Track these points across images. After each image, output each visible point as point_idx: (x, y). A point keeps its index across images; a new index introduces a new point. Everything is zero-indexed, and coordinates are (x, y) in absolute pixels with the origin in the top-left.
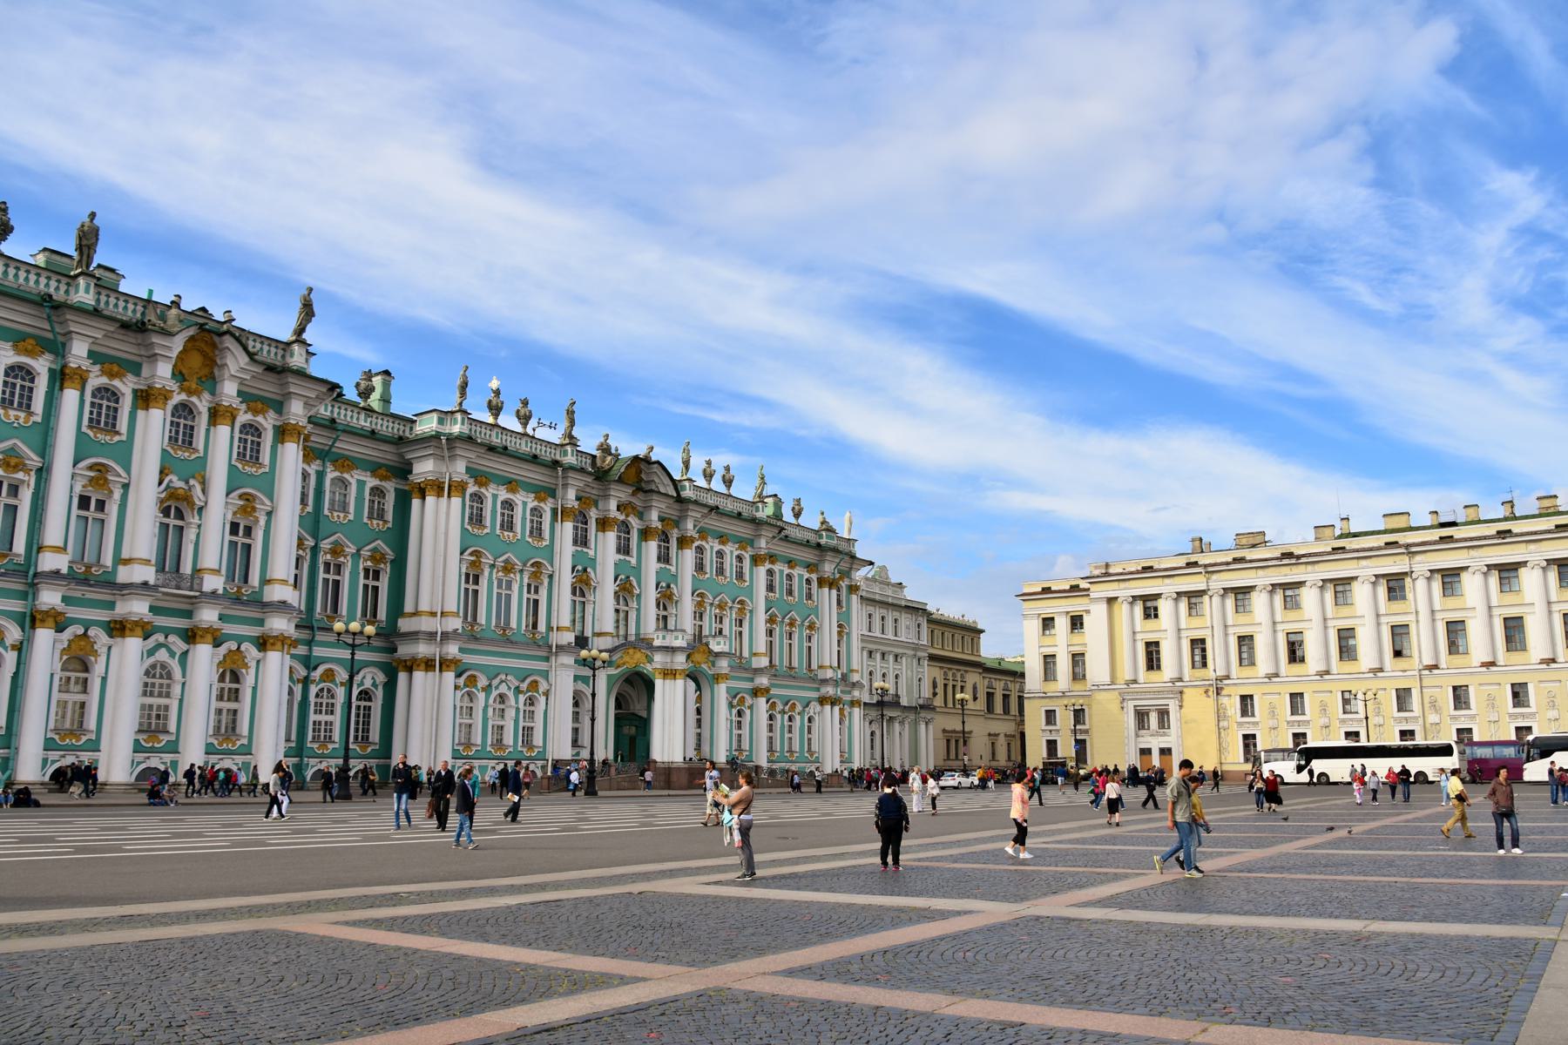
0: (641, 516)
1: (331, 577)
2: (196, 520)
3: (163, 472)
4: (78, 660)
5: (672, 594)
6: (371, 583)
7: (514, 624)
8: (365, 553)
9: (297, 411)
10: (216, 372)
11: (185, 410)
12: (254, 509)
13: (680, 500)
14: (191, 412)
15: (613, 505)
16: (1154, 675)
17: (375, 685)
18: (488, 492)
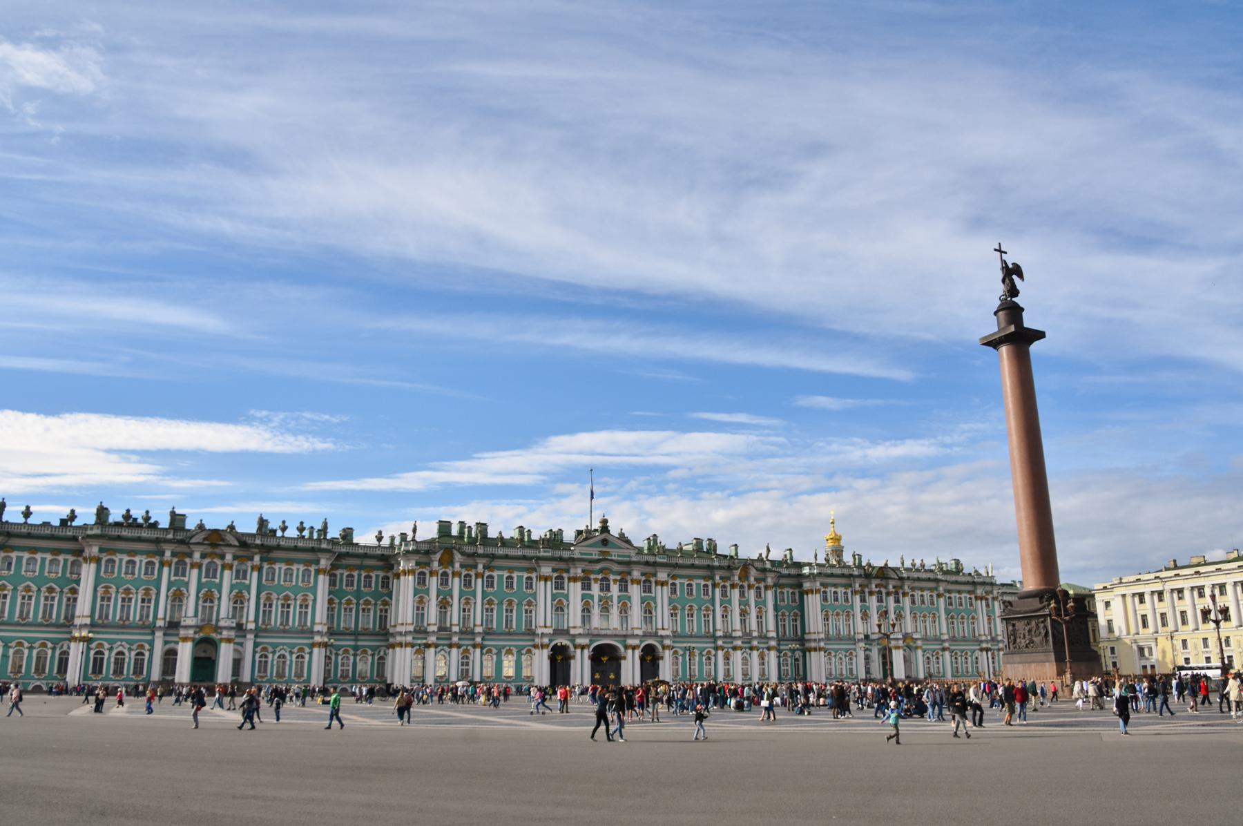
0: (886, 587)
4: (727, 658)
9: (770, 581)
11: (742, 587)
13: (901, 579)
16: (1146, 631)
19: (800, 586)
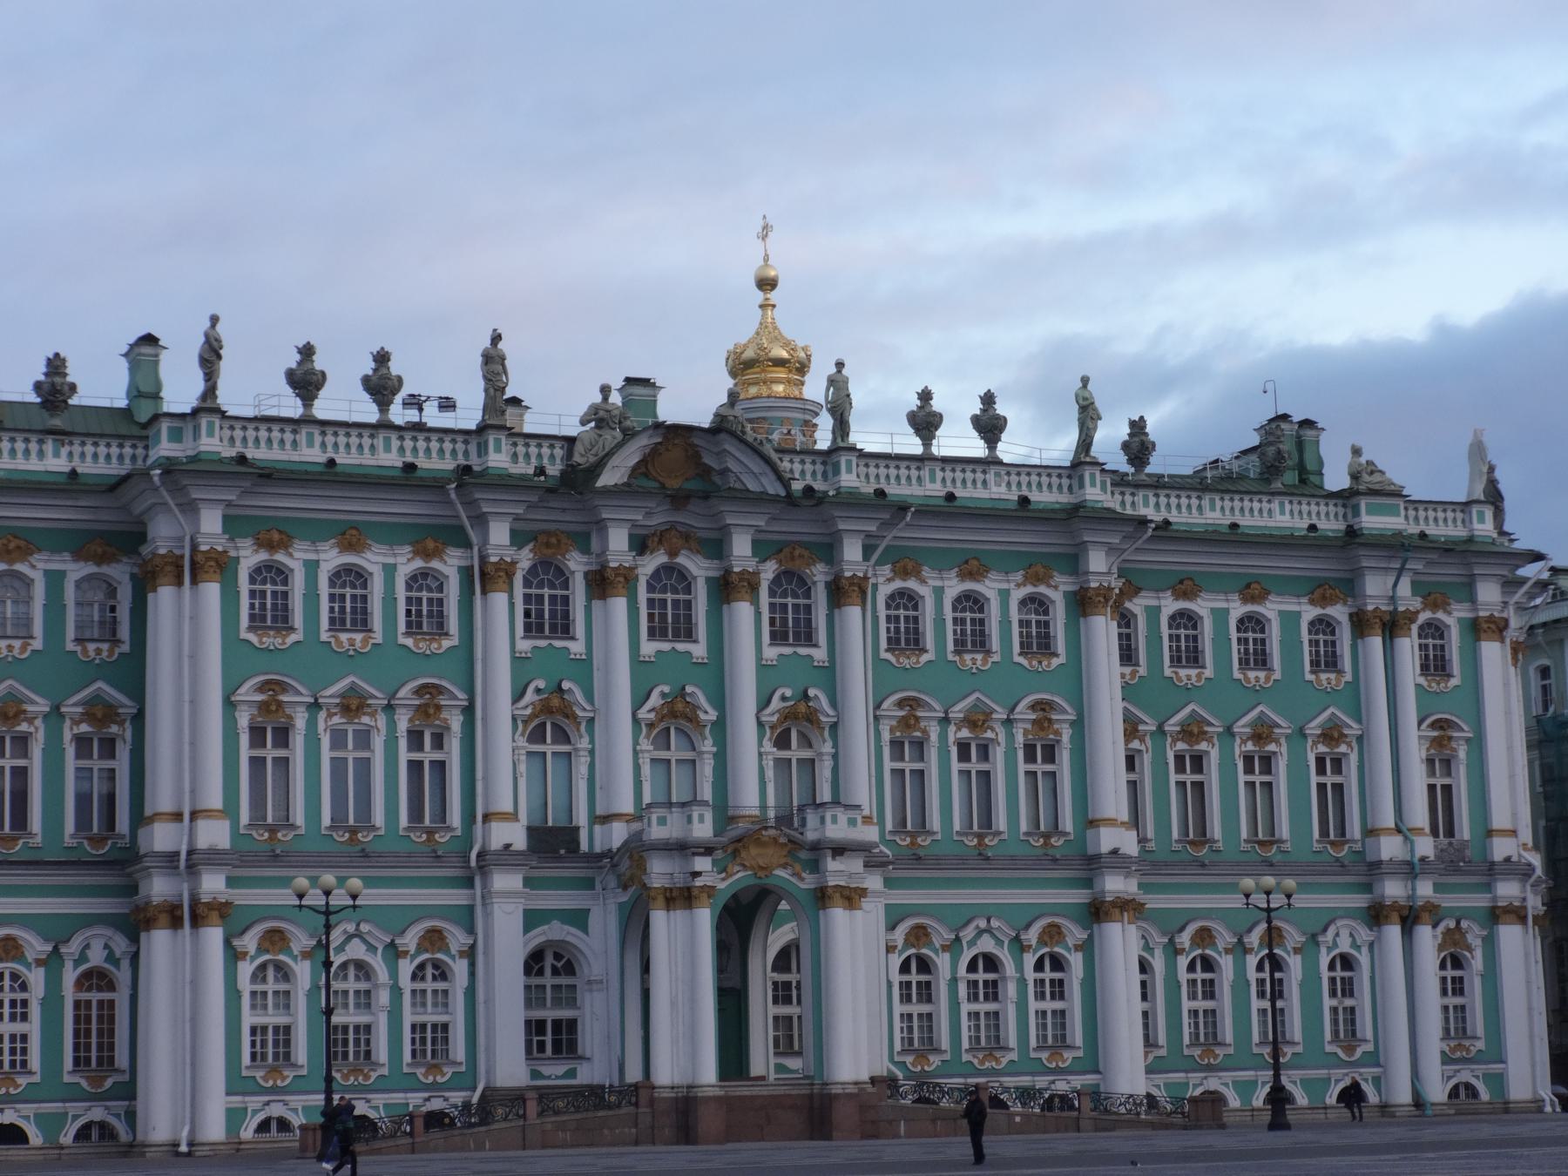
7: (379, 818)
8: (71, 708)
17: (111, 958)
18: (294, 560)
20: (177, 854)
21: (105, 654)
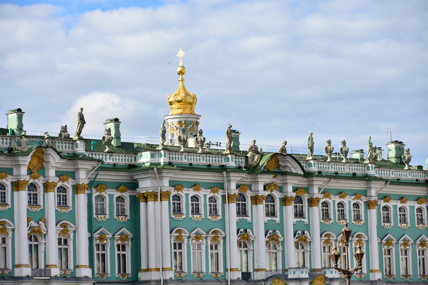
0: (281, 189)
1: (100, 252)
2: (44, 241)
3: (29, 220)
5: (306, 238)
6: (121, 253)
8: (117, 236)
10: (44, 164)
11: (33, 186)
12: (68, 231)
13: (308, 175)
14: (35, 187)
15: (261, 187)
18: (182, 194)
19: (134, 185)
20: (161, 280)
21: (124, 220)
